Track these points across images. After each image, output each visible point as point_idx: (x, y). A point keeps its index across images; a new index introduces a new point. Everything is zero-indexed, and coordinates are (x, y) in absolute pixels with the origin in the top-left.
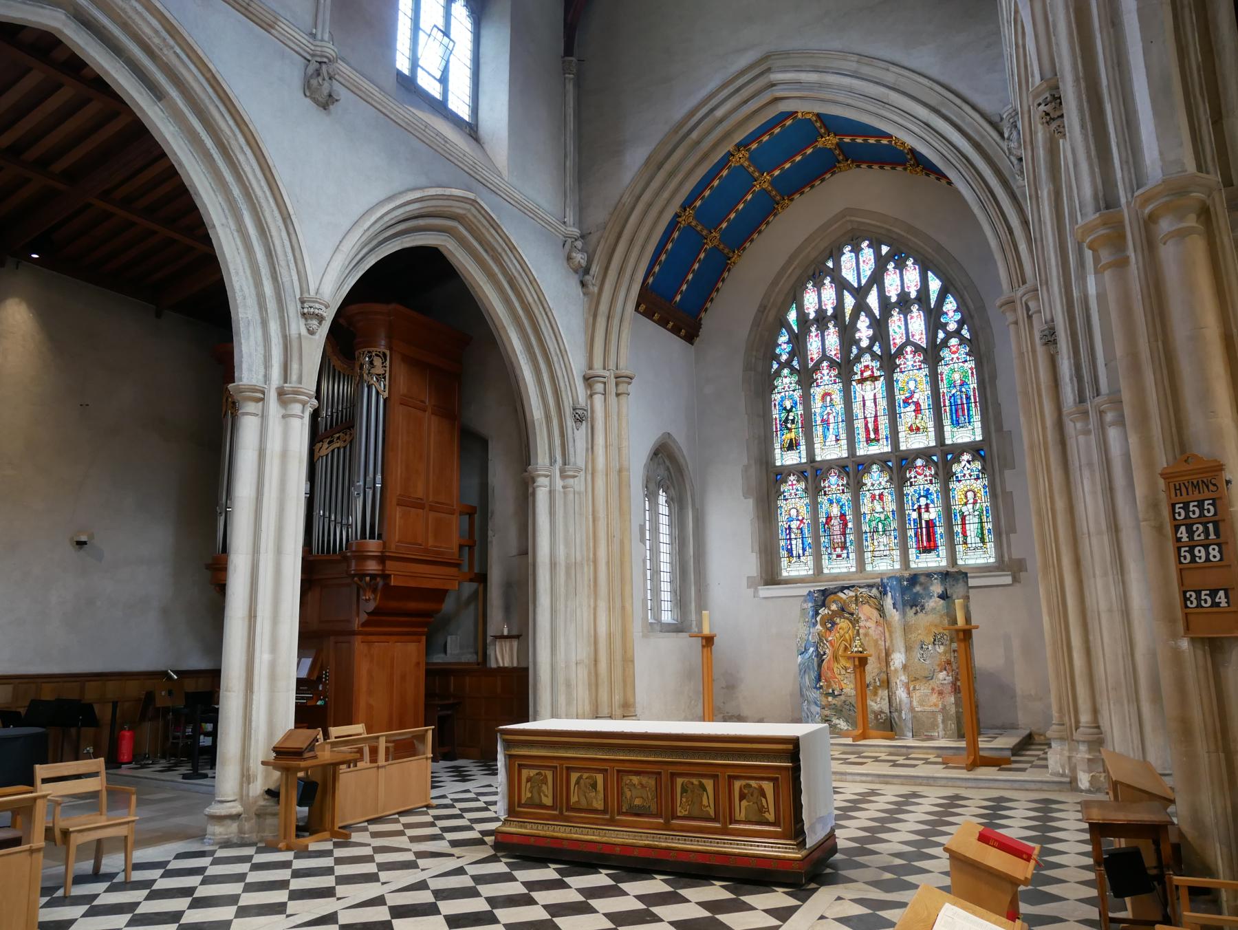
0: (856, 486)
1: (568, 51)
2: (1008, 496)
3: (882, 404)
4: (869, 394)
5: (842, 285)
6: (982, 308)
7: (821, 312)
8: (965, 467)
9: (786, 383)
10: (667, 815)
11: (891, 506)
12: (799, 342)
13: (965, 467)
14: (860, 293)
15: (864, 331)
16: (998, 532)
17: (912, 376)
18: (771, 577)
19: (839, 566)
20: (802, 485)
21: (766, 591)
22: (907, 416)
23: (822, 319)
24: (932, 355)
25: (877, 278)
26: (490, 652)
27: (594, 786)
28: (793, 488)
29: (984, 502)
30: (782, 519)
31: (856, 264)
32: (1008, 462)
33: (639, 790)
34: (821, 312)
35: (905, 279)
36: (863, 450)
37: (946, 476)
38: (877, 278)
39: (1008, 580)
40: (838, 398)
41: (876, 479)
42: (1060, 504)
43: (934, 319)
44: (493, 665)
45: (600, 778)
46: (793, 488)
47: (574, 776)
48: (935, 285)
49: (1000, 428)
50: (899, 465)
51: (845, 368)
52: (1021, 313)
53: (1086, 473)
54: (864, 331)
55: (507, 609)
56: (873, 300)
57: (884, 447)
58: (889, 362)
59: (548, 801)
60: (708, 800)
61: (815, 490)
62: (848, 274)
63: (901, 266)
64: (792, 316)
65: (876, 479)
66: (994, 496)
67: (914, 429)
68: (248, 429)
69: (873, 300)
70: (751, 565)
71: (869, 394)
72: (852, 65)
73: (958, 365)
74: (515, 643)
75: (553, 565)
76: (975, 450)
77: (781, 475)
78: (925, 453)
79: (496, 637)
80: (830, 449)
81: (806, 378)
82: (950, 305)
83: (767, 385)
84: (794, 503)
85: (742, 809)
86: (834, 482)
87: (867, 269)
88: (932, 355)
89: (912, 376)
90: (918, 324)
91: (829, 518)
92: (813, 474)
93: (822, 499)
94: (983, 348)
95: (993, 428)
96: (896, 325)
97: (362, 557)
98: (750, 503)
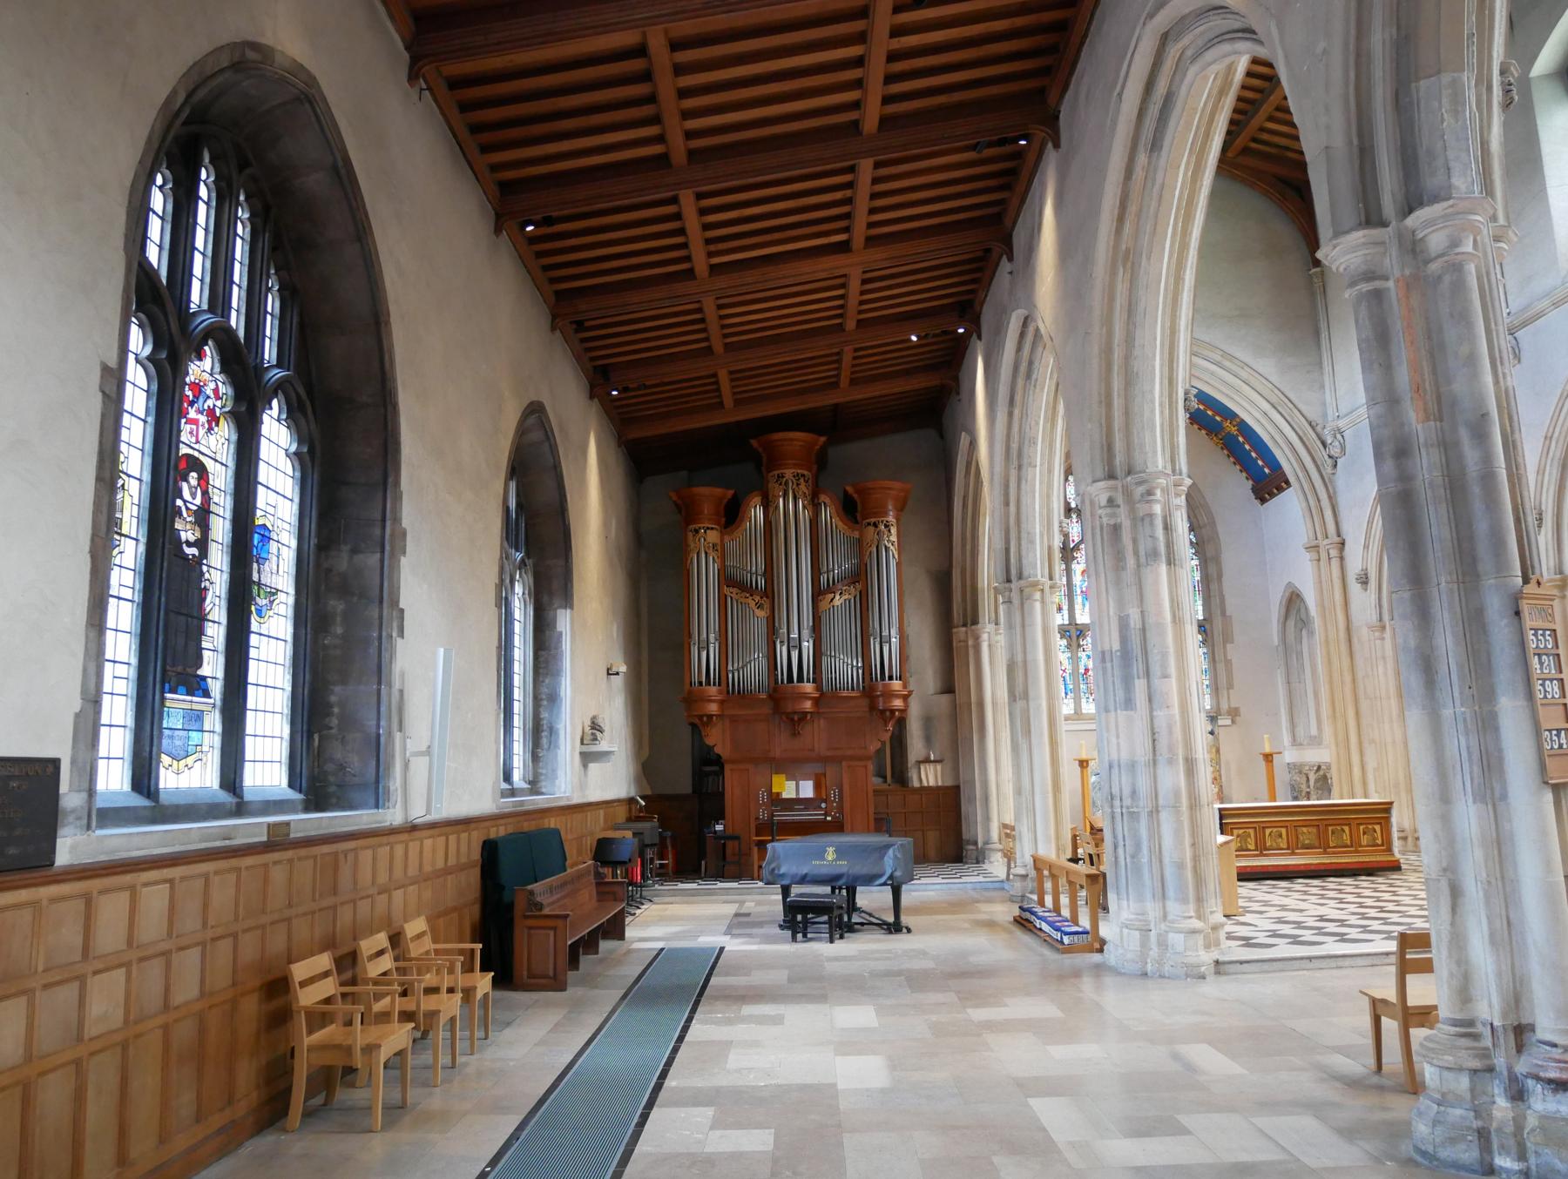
2: (1228, 663)
6: (1213, 524)
10: (1325, 847)
20: (1064, 642)
26: (913, 774)
27: (1280, 836)
32: (1228, 638)
33: (1307, 835)
39: (1228, 722)
42: (1348, 678)
44: (916, 784)
45: (1284, 831)
47: (1268, 831)
49: (1223, 613)
52: (1324, 556)
53: (1381, 664)
55: (928, 739)
59: (1252, 847)
60: (1346, 838)
66: (1213, 660)
72: (1218, 358)
74: (939, 767)
75: (994, 704)
79: (919, 763)
85: (1365, 840)
91: (1087, 670)
93: (1082, 654)
94: (1210, 552)
95: (1217, 612)
97: (890, 695)
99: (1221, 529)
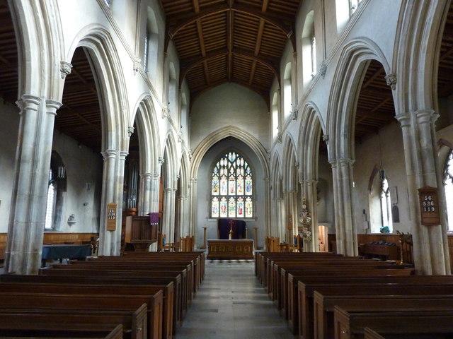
0: (228, 200)
1: (190, 113)
3: (235, 185)
4: (232, 183)
5: (228, 161)
7: (224, 166)
8: (249, 200)
9: (215, 179)
11: (234, 204)
12: (219, 171)
13: (249, 200)
14: (232, 163)
15: (232, 171)
16: (253, 212)
17: (240, 180)
18: (211, 217)
19: (224, 215)
21: (209, 220)
22: (239, 189)
23: (224, 167)
24: (244, 178)
25: (236, 160)
28: (215, 200)
29: (251, 206)
30: (213, 206)
31: (232, 156)
32: (256, 198)
34: (224, 166)
35: (241, 162)
36: (230, 194)
37: (245, 200)
38: (236, 160)
40: (226, 183)
41: (232, 200)
43: (245, 171)
46: (215, 200)
48: (246, 164)
50: (236, 198)
51: (228, 178)
54: (232, 171)
56: (234, 164)
57: (234, 194)
58: (236, 178)
61: (220, 200)
62: (230, 158)
63: (240, 159)
64: (218, 164)
65: (232, 200)
67: (240, 191)
68: (169, 194)
69: (234, 164)
70: (207, 215)
71: (232, 183)
73: (249, 180)
76: (250, 196)
77: (214, 196)
78: (241, 196)
80: (224, 193)
81: (220, 178)
82: (249, 169)
83: (211, 178)
84: (215, 202)
86: (224, 200)
87: (234, 158)
88: (244, 178)
89: (240, 180)
90: (242, 171)
92: (220, 197)
96: (238, 170)
98: (207, 202)
99: (257, 173)
